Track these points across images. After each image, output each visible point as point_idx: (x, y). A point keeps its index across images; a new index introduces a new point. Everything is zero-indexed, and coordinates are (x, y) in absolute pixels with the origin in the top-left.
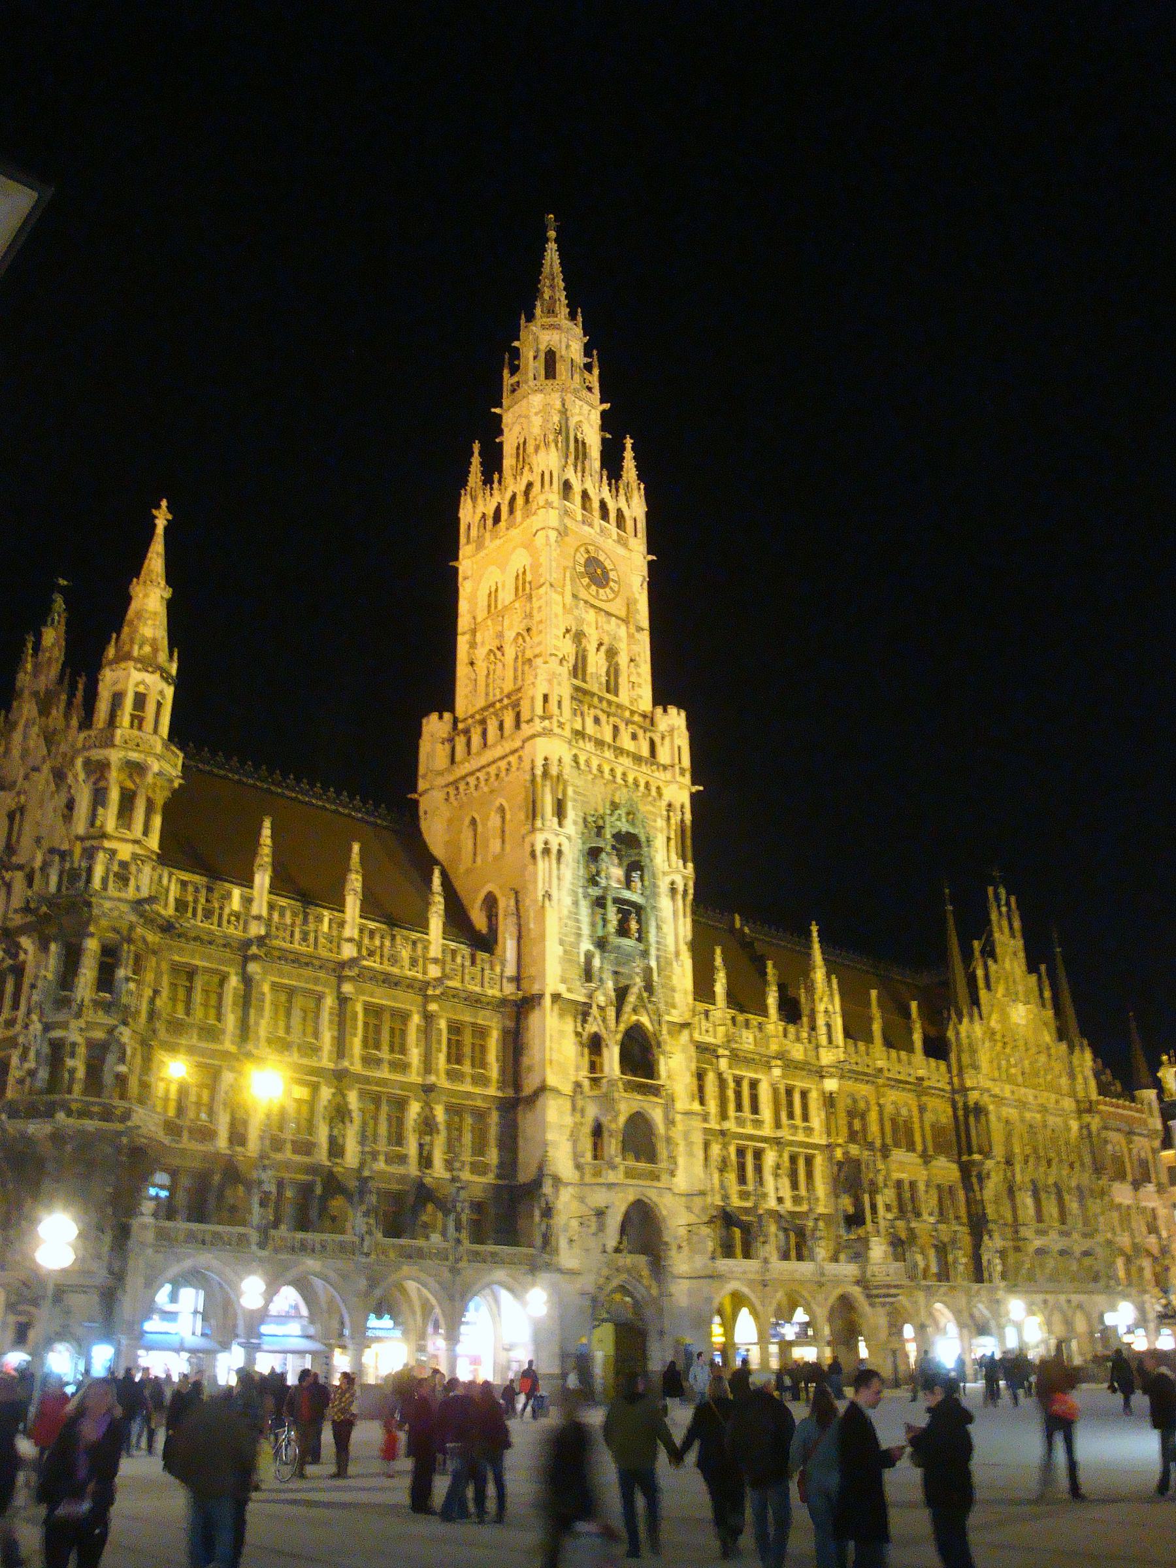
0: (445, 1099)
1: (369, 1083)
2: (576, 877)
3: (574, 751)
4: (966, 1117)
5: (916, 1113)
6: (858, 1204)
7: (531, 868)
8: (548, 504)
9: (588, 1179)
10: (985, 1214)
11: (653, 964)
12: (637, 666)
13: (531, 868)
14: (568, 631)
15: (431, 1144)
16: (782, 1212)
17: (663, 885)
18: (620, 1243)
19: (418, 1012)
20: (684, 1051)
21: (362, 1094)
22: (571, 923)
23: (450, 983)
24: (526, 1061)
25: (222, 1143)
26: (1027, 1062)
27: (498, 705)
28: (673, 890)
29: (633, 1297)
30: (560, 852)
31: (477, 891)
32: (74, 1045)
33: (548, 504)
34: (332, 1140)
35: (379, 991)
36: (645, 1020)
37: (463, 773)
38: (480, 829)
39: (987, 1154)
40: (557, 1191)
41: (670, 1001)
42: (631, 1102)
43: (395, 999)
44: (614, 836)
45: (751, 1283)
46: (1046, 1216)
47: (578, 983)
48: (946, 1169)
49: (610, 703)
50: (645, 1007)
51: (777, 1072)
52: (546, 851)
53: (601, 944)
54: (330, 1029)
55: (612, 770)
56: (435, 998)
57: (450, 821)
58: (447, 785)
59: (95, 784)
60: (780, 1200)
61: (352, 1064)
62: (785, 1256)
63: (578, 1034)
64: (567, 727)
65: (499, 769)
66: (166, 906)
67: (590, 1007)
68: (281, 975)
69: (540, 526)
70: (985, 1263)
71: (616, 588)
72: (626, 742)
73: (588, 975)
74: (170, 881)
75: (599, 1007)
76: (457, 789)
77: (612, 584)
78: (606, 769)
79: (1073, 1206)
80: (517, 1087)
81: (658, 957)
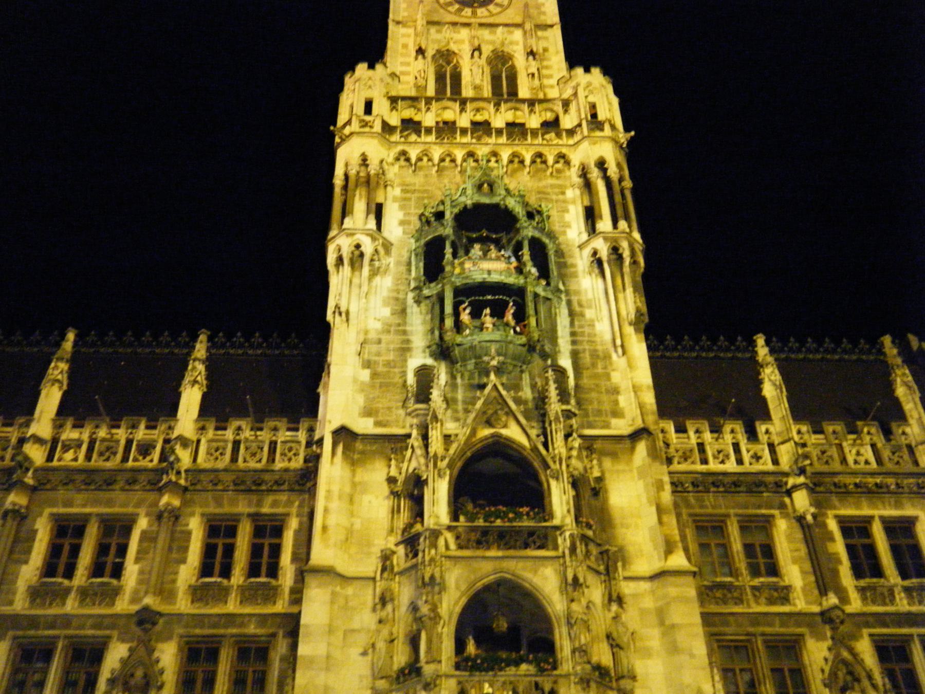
1: (37, 627)
3: (400, 148)
11: (565, 362)
14: (420, 51)
19: (147, 515)
20: (642, 474)
35: (79, 498)
36: (513, 432)
41: (606, 407)
43: (109, 503)
47: (402, 412)
50: (510, 413)
61: (11, 603)
63: (391, 480)
67: (409, 436)
81: (575, 355)
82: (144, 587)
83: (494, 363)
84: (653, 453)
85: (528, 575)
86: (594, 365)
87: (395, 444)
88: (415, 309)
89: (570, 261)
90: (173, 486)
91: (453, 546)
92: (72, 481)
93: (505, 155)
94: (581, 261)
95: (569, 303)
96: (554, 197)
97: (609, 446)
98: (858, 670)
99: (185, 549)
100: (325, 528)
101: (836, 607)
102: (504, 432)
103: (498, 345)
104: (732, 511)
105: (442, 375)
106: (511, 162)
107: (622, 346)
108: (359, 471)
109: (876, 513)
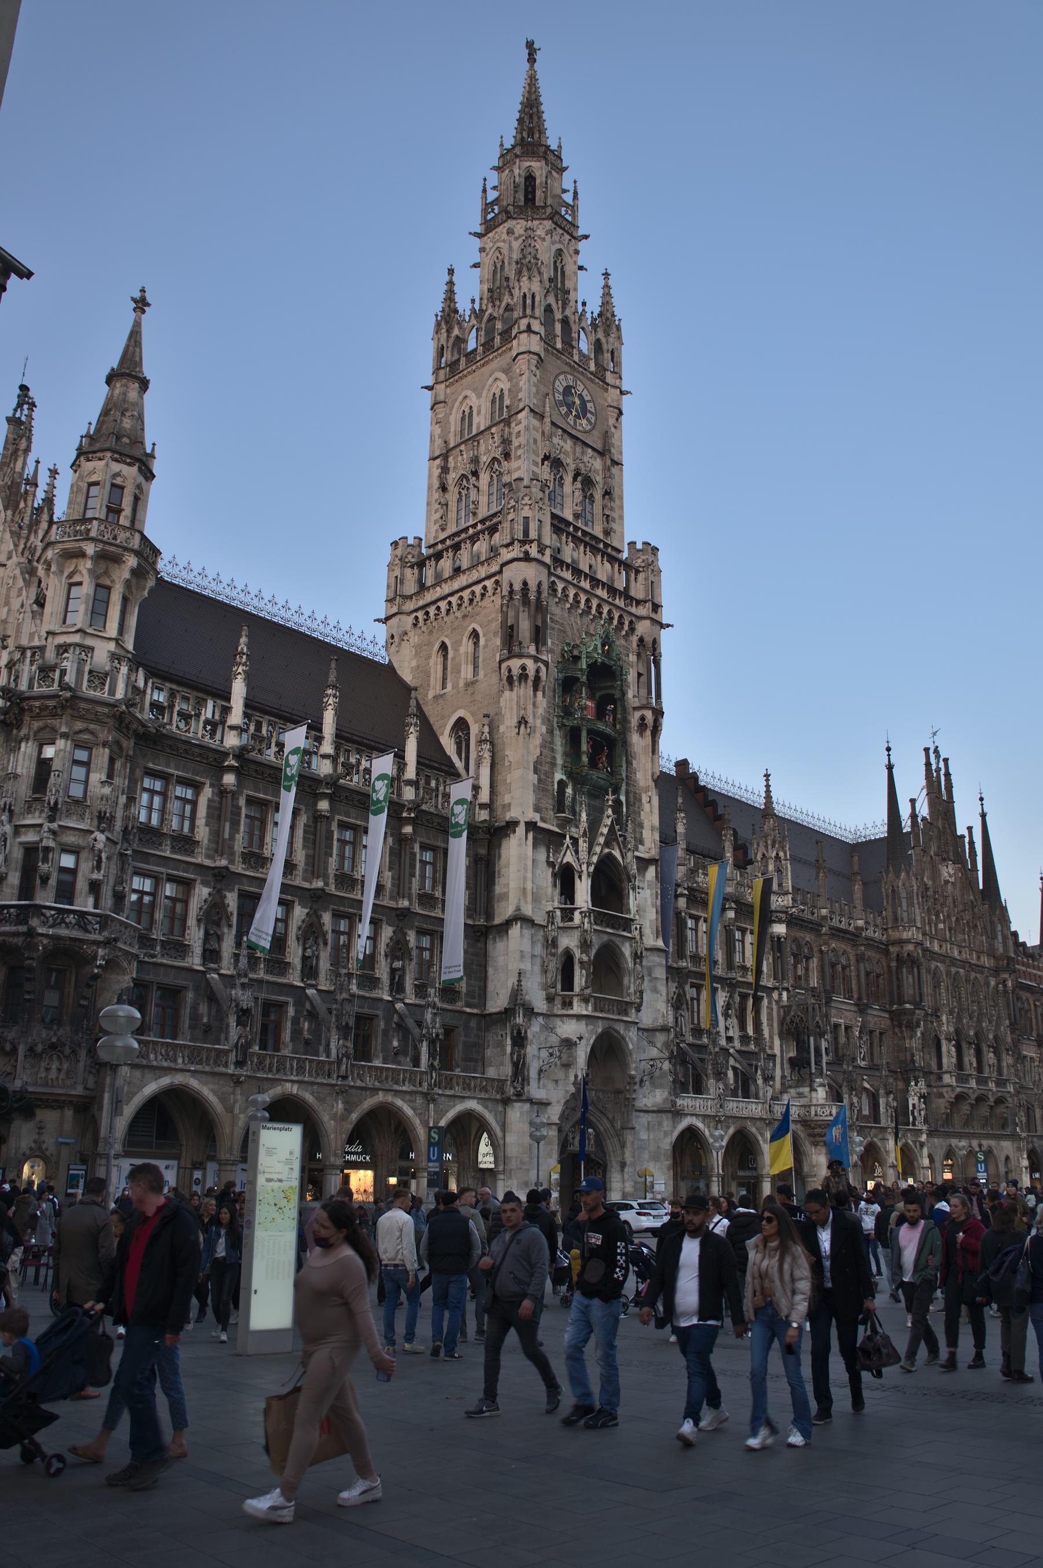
2: (551, 705)
3: (553, 578)
4: (899, 968)
5: (853, 962)
6: (802, 1047)
7: (507, 693)
8: (529, 330)
9: (558, 1010)
10: (913, 1061)
11: (623, 798)
12: (611, 499)
13: (507, 693)
14: (546, 458)
15: (403, 969)
16: (731, 1051)
17: (634, 719)
18: (587, 1075)
21: (337, 915)
22: (545, 751)
23: (424, 807)
24: (498, 889)
25: (195, 961)
26: (953, 919)
27: (471, 531)
28: (642, 726)
30: (537, 679)
31: (444, 718)
32: (47, 850)
33: (529, 330)
34: (304, 958)
35: (353, 811)
36: (617, 853)
37: (434, 598)
38: (450, 655)
39: (918, 1004)
40: (530, 1020)
41: (638, 836)
42: (602, 935)
44: (589, 666)
45: (705, 1117)
46: (967, 1065)
48: (878, 1018)
49: (585, 533)
52: (523, 676)
53: (574, 775)
54: (304, 847)
55: (588, 601)
56: (408, 821)
57: (418, 648)
58: (416, 610)
59: (70, 576)
60: (730, 1039)
61: (327, 884)
62: (734, 1093)
63: (551, 864)
64: (548, 552)
65: (473, 593)
66: (142, 710)
67: (564, 836)
69: (522, 350)
70: (911, 1108)
71: (593, 421)
72: (602, 576)
73: (560, 806)
74: (146, 683)
75: (571, 838)
76: (427, 613)
77: (589, 415)
78: (583, 598)
79: (990, 1057)
80: (489, 915)
82: (396, 890)
85: (620, 944)
89: (629, 717)
109: (703, 915)
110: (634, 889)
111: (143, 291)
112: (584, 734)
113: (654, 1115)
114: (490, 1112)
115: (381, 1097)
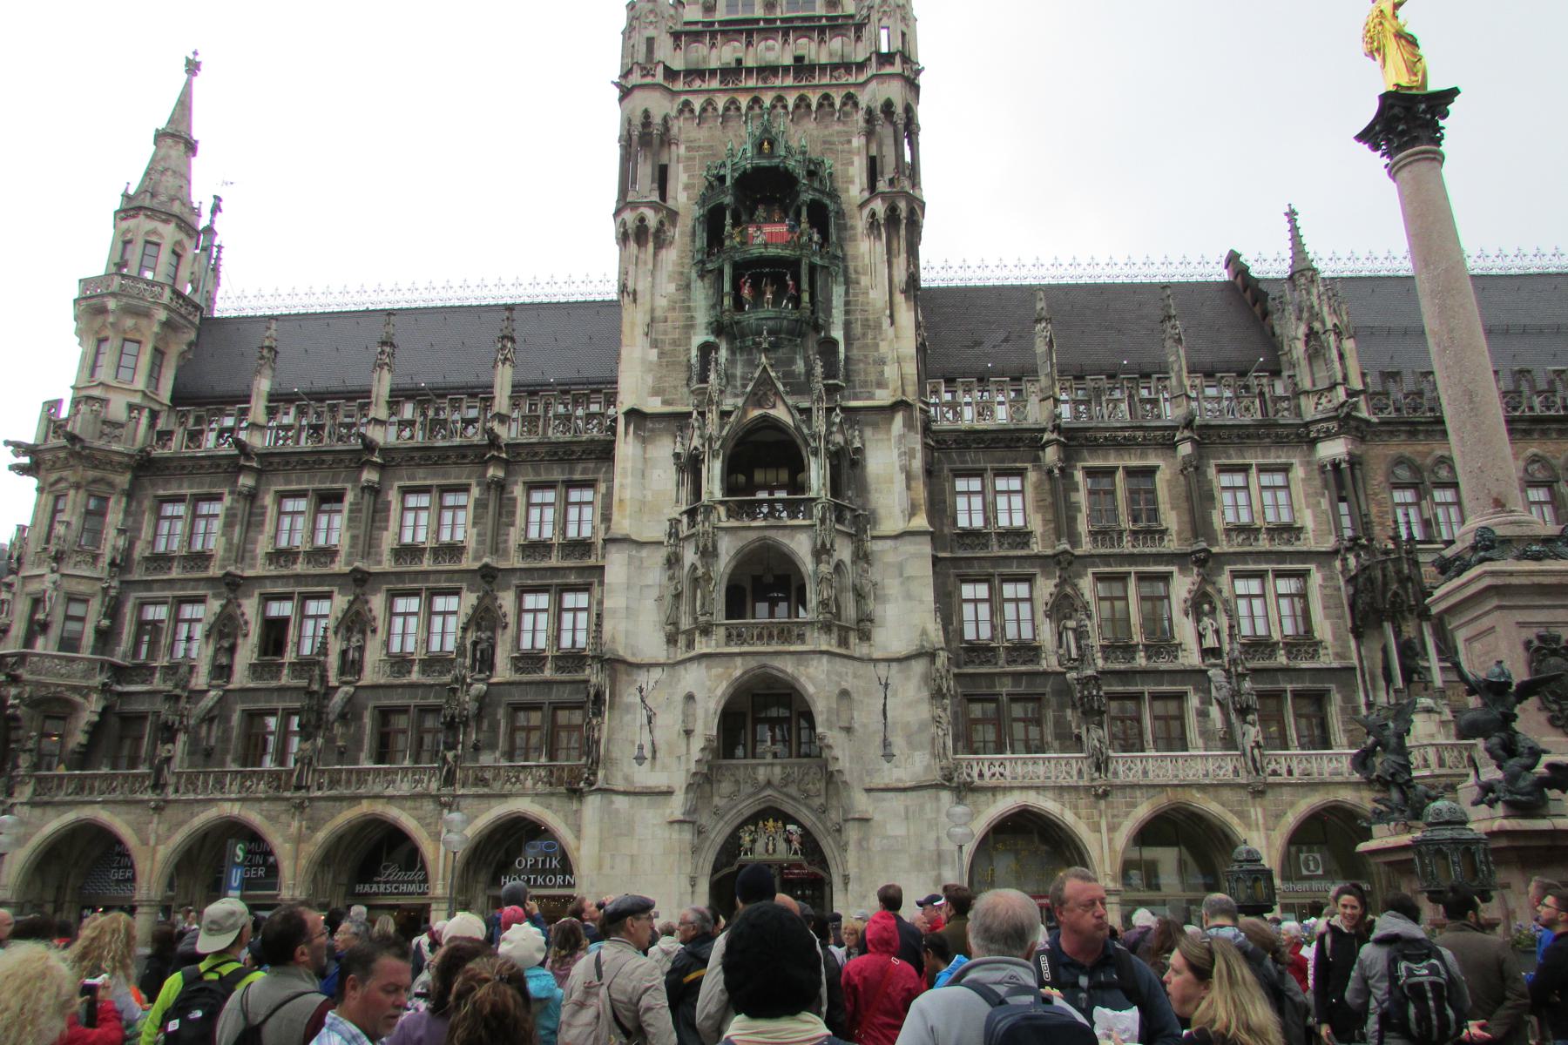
0: (517, 582)
3: (683, 98)
11: (837, 333)
28: (873, 225)
29: (800, 825)
35: (421, 472)
36: (780, 413)
41: (873, 378)
42: (743, 533)
43: (445, 476)
47: (686, 390)
50: (777, 393)
51: (1185, 449)
61: (379, 563)
63: (677, 456)
68: (288, 482)
81: (847, 326)
83: (765, 345)
84: (909, 425)
85: (786, 541)
86: (864, 335)
87: (678, 421)
88: (699, 283)
89: (850, 222)
90: (497, 460)
91: (723, 518)
92: (412, 458)
93: (791, 101)
94: (860, 223)
95: (846, 269)
96: (840, 147)
97: (873, 417)
98: (1078, 603)
99: (513, 513)
100: (621, 501)
101: (1065, 552)
102: (771, 412)
103: (770, 323)
104: (989, 466)
105: (723, 353)
106: (797, 107)
107: (892, 316)
108: (650, 447)
109: (1121, 463)
110: (816, 453)
111: (195, 53)
112: (727, 270)
113: (914, 794)
114: (555, 812)
115: (365, 808)
